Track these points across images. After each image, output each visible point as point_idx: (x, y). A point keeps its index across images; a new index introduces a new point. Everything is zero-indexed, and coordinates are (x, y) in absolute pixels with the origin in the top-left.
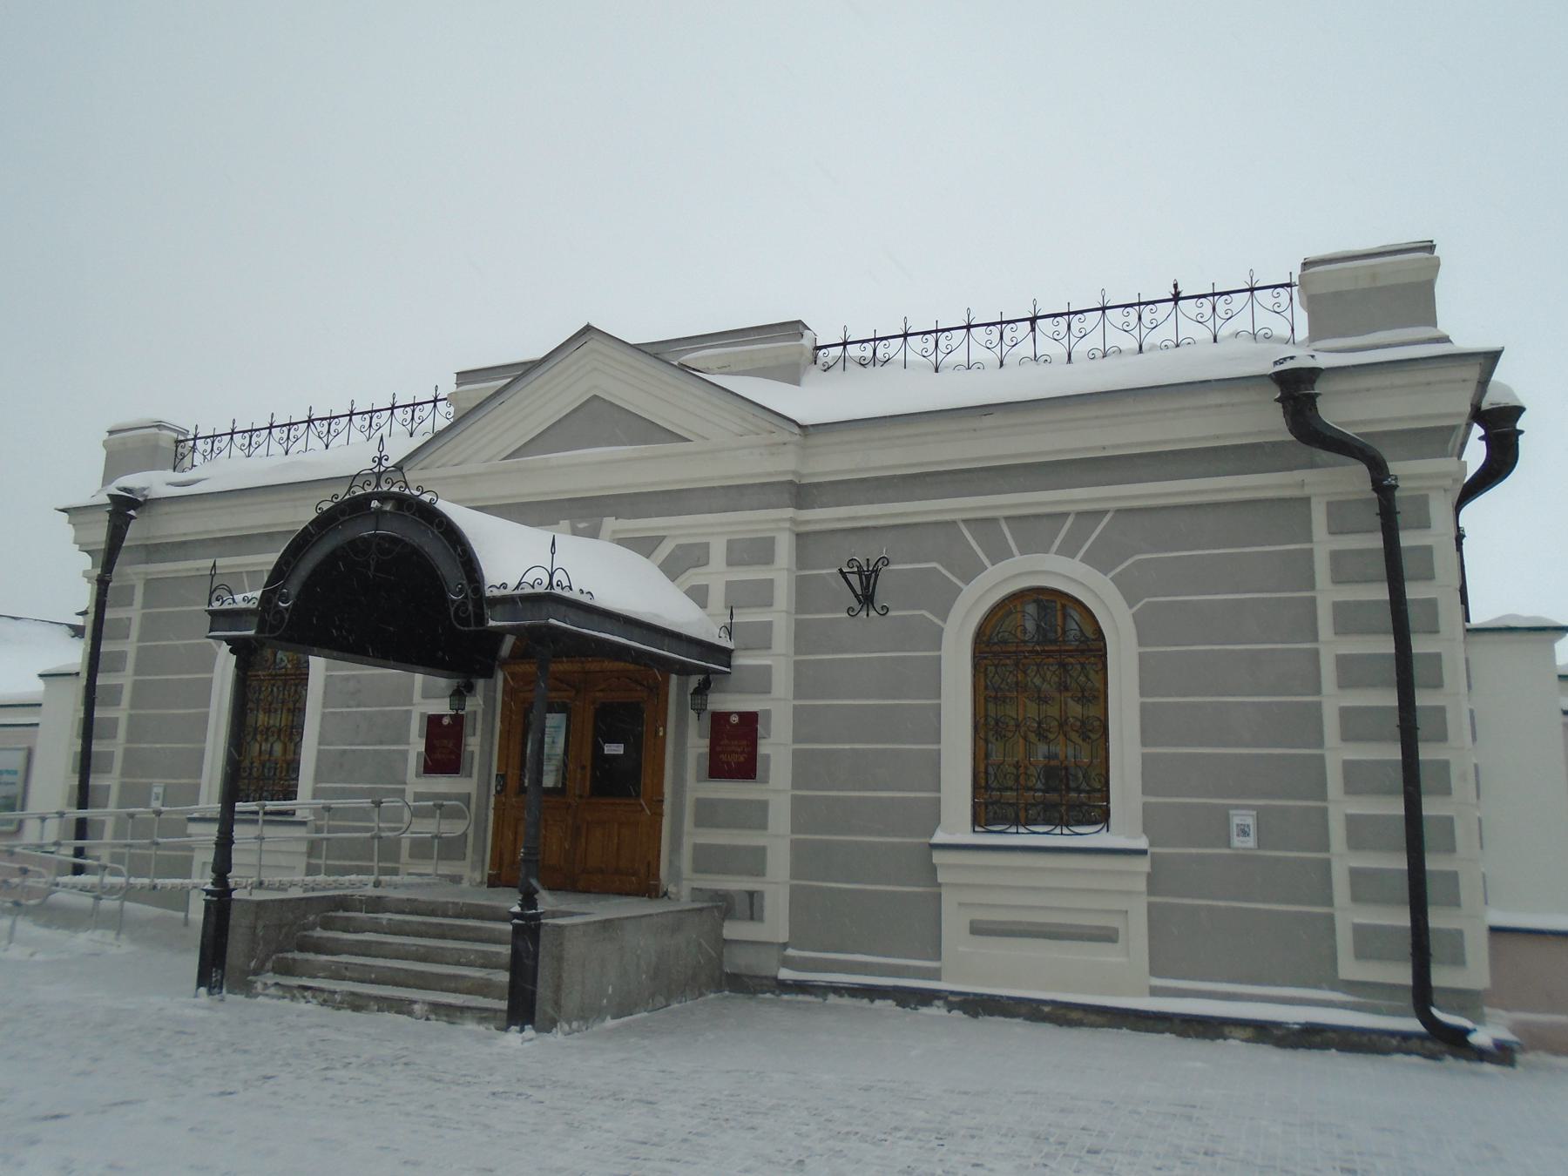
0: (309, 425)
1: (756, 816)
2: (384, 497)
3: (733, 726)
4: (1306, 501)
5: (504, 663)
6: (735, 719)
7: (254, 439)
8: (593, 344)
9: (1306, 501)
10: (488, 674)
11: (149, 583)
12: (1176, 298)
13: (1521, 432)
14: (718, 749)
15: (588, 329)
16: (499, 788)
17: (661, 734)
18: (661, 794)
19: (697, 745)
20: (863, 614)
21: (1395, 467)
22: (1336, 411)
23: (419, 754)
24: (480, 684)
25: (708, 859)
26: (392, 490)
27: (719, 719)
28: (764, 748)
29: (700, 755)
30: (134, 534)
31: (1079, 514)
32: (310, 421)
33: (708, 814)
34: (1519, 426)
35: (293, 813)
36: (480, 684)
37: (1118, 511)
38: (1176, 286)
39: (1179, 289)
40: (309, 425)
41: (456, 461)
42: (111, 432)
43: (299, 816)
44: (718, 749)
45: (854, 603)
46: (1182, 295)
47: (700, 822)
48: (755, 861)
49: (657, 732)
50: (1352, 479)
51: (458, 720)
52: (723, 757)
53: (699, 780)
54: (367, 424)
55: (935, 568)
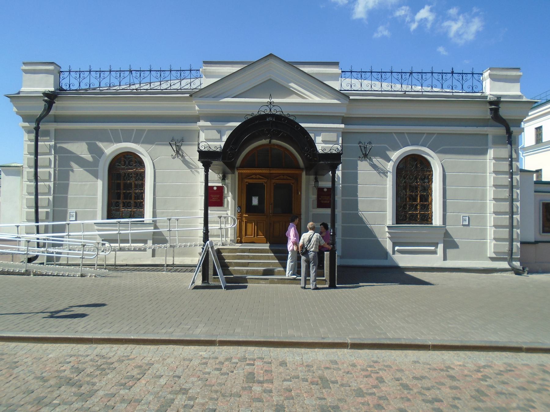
3: (325, 192)
4: (487, 135)
5: (238, 168)
6: (325, 190)
8: (272, 61)
9: (487, 135)
12: (453, 73)
14: (320, 199)
15: (271, 55)
16: (239, 211)
17: (300, 194)
18: (300, 212)
19: (313, 197)
21: (512, 129)
22: (504, 112)
24: (230, 176)
29: (313, 200)
31: (427, 133)
35: (143, 221)
37: (438, 133)
38: (453, 69)
44: (320, 199)
46: (454, 72)
50: (501, 131)
51: (220, 189)
52: (322, 202)
53: (313, 208)
55: (385, 146)
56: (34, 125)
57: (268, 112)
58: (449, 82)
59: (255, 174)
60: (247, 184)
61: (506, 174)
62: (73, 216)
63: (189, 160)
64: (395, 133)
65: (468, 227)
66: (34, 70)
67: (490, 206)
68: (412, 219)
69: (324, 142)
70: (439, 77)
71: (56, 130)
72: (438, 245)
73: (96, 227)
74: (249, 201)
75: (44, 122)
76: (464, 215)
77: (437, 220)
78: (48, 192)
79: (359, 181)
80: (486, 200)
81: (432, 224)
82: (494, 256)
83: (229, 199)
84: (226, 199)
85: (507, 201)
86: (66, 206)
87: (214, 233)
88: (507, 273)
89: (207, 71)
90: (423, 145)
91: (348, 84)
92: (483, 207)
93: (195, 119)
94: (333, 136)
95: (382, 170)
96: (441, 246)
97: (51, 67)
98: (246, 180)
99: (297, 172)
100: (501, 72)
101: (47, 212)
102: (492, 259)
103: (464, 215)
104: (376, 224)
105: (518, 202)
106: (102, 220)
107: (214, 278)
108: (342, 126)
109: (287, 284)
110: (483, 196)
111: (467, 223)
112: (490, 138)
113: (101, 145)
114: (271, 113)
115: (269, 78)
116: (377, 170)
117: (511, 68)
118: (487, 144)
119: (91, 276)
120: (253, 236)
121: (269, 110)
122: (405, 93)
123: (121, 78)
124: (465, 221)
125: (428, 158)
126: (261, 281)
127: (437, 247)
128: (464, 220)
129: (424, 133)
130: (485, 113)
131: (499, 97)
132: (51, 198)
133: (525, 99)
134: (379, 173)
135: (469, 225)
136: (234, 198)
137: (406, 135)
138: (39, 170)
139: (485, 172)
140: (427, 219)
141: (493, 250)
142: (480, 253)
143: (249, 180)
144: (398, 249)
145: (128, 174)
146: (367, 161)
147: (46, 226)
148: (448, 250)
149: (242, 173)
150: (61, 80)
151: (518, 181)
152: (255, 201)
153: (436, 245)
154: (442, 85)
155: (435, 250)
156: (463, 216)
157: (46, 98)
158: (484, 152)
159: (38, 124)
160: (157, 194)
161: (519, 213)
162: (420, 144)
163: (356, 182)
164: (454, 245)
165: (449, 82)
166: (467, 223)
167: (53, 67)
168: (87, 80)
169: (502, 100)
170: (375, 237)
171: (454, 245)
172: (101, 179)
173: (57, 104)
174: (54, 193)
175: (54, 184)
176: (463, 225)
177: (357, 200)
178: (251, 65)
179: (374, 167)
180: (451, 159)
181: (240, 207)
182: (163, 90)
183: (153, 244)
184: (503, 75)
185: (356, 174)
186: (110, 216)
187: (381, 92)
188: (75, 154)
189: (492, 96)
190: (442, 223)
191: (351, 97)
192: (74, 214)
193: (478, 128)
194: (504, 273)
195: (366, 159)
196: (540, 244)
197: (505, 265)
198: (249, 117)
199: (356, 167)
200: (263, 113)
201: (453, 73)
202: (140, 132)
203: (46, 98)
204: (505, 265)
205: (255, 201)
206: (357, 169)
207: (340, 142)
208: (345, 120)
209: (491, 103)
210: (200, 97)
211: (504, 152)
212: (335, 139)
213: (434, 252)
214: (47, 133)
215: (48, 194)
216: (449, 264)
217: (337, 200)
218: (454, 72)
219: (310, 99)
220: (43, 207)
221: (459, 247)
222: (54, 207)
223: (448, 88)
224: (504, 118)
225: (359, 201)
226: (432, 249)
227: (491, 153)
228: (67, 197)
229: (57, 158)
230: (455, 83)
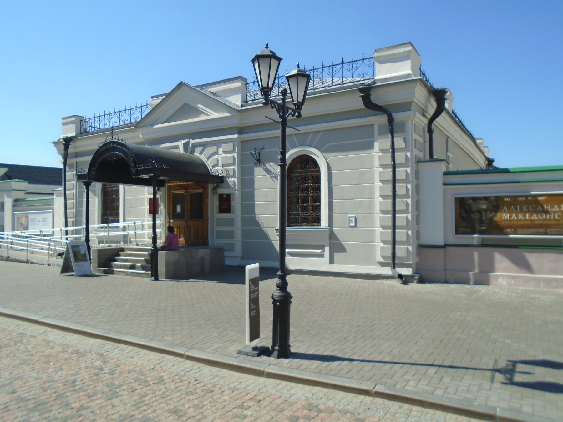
0: (114, 114)
1: (231, 222)
4: (373, 125)
6: (225, 196)
7: (101, 119)
8: (183, 88)
9: (373, 125)
10: (163, 186)
12: (343, 63)
13: (446, 99)
17: (207, 201)
19: (217, 203)
20: (258, 164)
22: (375, 98)
25: (221, 235)
27: (221, 196)
28: (232, 203)
30: (71, 150)
31: (314, 132)
32: (115, 113)
33: (221, 222)
34: (446, 97)
35: (119, 227)
36: (162, 188)
37: (324, 131)
38: (343, 60)
40: (114, 114)
41: (150, 124)
42: (63, 119)
43: (120, 228)
45: (257, 162)
47: (217, 225)
48: (231, 235)
49: (206, 200)
50: (383, 119)
54: (140, 110)
55: (276, 150)
58: (360, 70)
59: (178, 186)
60: (191, 194)
61: (389, 168)
65: (355, 229)
68: (306, 221)
69: (225, 152)
72: (324, 248)
73: (94, 232)
74: (175, 209)
77: (324, 223)
79: (256, 185)
82: (382, 260)
84: (160, 208)
85: (389, 199)
88: (393, 280)
89: (152, 104)
90: (310, 146)
92: (371, 206)
94: (229, 147)
95: (274, 174)
96: (327, 249)
97: (73, 119)
100: (386, 52)
101: (73, 221)
104: (270, 226)
105: (409, 198)
107: (98, 269)
108: (236, 136)
110: (371, 194)
111: (353, 225)
112: (376, 129)
116: (270, 174)
117: (404, 44)
118: (373, 136)
119: (52, 265)
124: (352, 221)
125: (315, 157)
126: (122, 274)
128: (350, 221)
129: (310, 133)
130: (357, 102)
132: (74, 211)
133: (414, 78)
134: (272, 177)
135: (356, 226)
136: (165, 208)
137: (294, 136)
138: (67, 192)
139: (372, 167)
140: (317, 221)
142: (368, 259)
144: (287, 251)
146: (261, 166)
147: (72, 231)
148: (335, 254)
149: (170, 186)
151: (409, 174)
152: (179, 209)
153: (322, 247)
154: (353, 75)
155: (322, 253)
158: (370, 146)
160: (126, 206)
161: (410, 211)
162: (307, 143)
163: (253, 188)
164: (342, 249)
165: (360, 70)
166: (353, 225)
167: (75, 118)
170: (270, 239)
171: (342, 249)
173: (72, 145)
174: (76, 208)
175: (76, 201)
176: (350, 226)
177: (254, 204)
178: (168, 95)
179: (268, 171)
180: (335, 157)
181: (169, 214)
183: (124, 243)
184: (389, 55)
185: (253, 180)
190: (328, 225)
193: (350, 120)
194: (390, 280)
195: (261, 164)
197: (387, 271)
199: (252, 173)
204: (387, 271)
205: (179, 209)
206: (253, 175)
207: (236, 151)
208: (241, 131)
212: (232, 149)
213: (321, 256)
214: (71, 167)
215: (73, 208)
216: (335, 268)
218: (344, 62)
220: (71, 218)
221: (347, 251)
222: (76, 217)
224: (380, 104)
225: (255, 205)
226: (319, 252)
227: (377, 145)
230: (366, 69)
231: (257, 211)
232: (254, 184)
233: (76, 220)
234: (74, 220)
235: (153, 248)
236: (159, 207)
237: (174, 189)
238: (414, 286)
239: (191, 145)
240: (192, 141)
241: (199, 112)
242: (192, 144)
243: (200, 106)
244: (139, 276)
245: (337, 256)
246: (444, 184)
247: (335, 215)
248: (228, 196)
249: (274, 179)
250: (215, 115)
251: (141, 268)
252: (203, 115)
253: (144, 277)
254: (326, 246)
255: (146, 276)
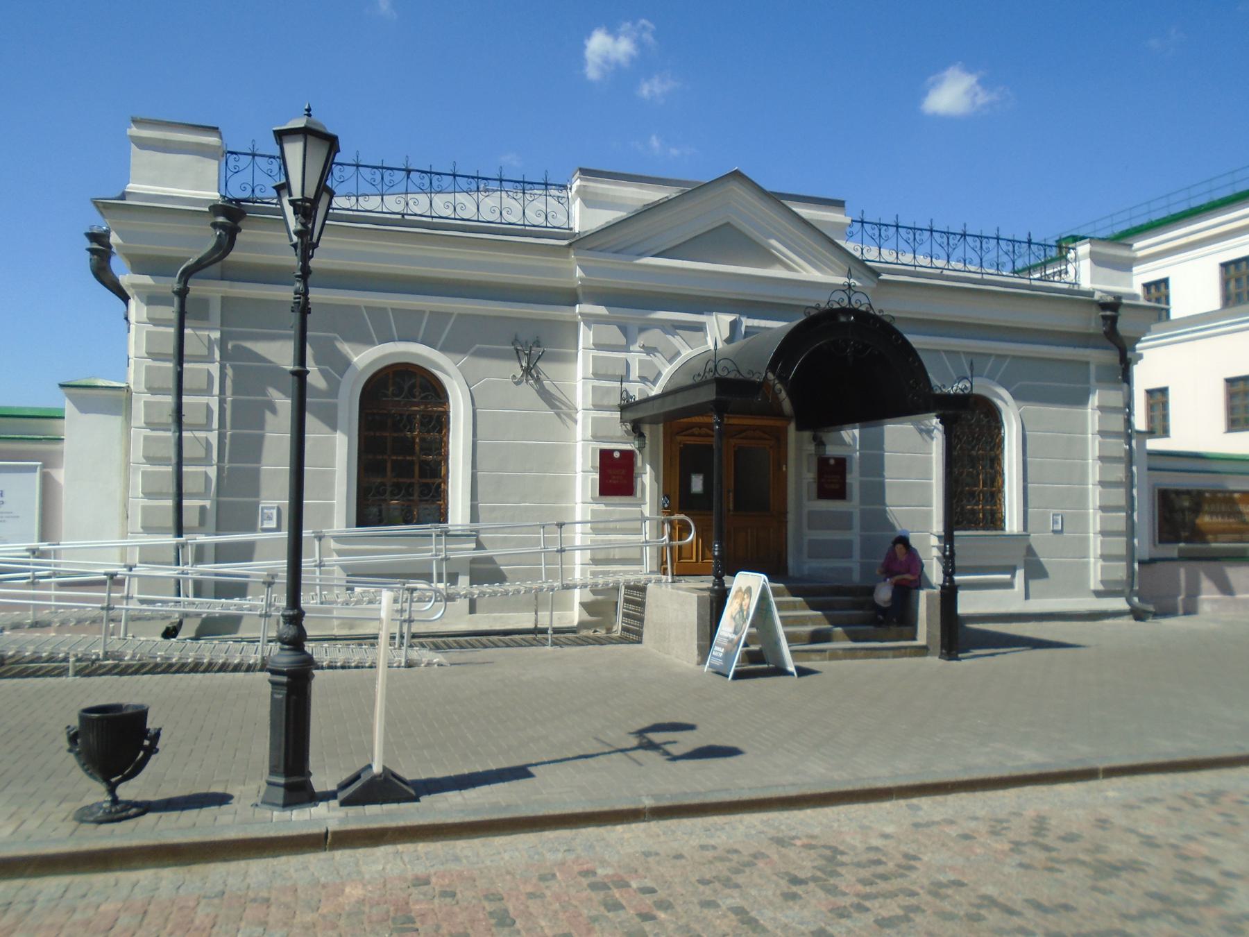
2: (855, 312)
6: (832, 462)
9: (1087, 363)
11: (225, 301)
15: (737, 175)
16: (666, 506)
17: (784, 469)
19: (810, 476)
22: (1124, 326)
23: (593, 480)
25: (818, 550)
26: (860, 308)
33: (817, 521)
37: (1014, 357)
38: (1030, 235)
39: (1032, 237)
47: (809, 528)
50: (1109, 357)
51: (628, 456)
53: (809, 499)
56: (173, 283)
57: (845, 304)
62: (270, 518)
63: (553, 390)
64: (946, 352)
66: (165, 141)
67: (1094, 496)
70: (874, 232)
71: (225, 301)
74: (686, 484)
75: (195, 278)
76: (1055, 511)
77: (1013, 524)
78: (204, 456)
79: (887, 446)
80: (1087, 484)
81: (1003, 529)
82: (1100, 587)
83: (647, 479)
84: (639, 479)
86: (256, 492)
87: (614, 556)
91: (540, 212)
93: (571, 298)
96: (1020, 574)
97: (212, 140)
98: (679, 438)
99: (779, 423)
101: (203, 508)
102: (1098, 594)
103: (1055, 511)
104: (915, 530)
106: (358, 525)
109: (861, 658)
110: (1083, 480)
113: (346, 348)
114: (851, 307)
115: (724, 221)
118: (1087, 381)
120: (694, 560)
121: (846, 301)
122: (942, 272)
123: (229, 172)
125: (999, 403)
126: (813, 656)
127: (1013, 576)
128: (1055, 522)
129: (990, 355)
130: (1093, 323)
131: (1118, 297)
135: (1061, 531)
137: (962, 356)
138: (185, 399)
139: (1084, 432)
141: (1099, 578)
142: (1079, 586)
143: (687, 438)
145: (409, 416)
150: (229, 174)
152: (697, 484)
153: (1012, 570)
156: (1053, 515)
157: (221, 219)
159: (186, 282)
160: (479, 466)
163: (882, 448)
168: (245, 177)
169: (1124, 301)
172: (343, 431)
176: (1054, 531)
180: (1033, 408)
181: (667, 495)
182: (436, 217)
183: (472, 583)
186: (362, 521)
187: (913, 268)
188: (270, 362)
189: (1104, 294)
190: (1021, 529)
191: (884, 277)
192: (275, 512)
196: (1159, 565)
197: (1120, 604)
198: (813, 312)
200: (836, 306)
201: (1030, 242)
202: (439, 317)
203: (221, 219)
204: (1120, 604)
205: (697, 484)
209: (1104, 306)
210: (588, 249)
211: (1115, 398)
213: (1009, 585)
215: (206, 461)
217: (851, 484)
218: (1033, 241)
219: (804, 273)
220: (193, 496)
223: (991, 266)
226: (1007, 579)
227: (1094, 400)
228: (257, 472)
229: (229, 372)
231: (889, 498)
232: (883, 443)
233: (219, 505)
234: (208, 503)
235: (716, 587)
236: (636, 478)
237: (684, 433)
238: (1149, 626)
239: (743, 329)
240: (747, 322)
241: (770, 258)
242: (747, 327)
243: (773, 242)
244: (870, 658)
245: (1033, 584)
246: (1150, 469)
247: (1030, 510)
248: (842, 463)
249: (925, 436)
250: (810, 274)
251: (846, 637)
252: (779, 266)
253: (886, 657)
254: (1021, 568)
255: (891, 653)
